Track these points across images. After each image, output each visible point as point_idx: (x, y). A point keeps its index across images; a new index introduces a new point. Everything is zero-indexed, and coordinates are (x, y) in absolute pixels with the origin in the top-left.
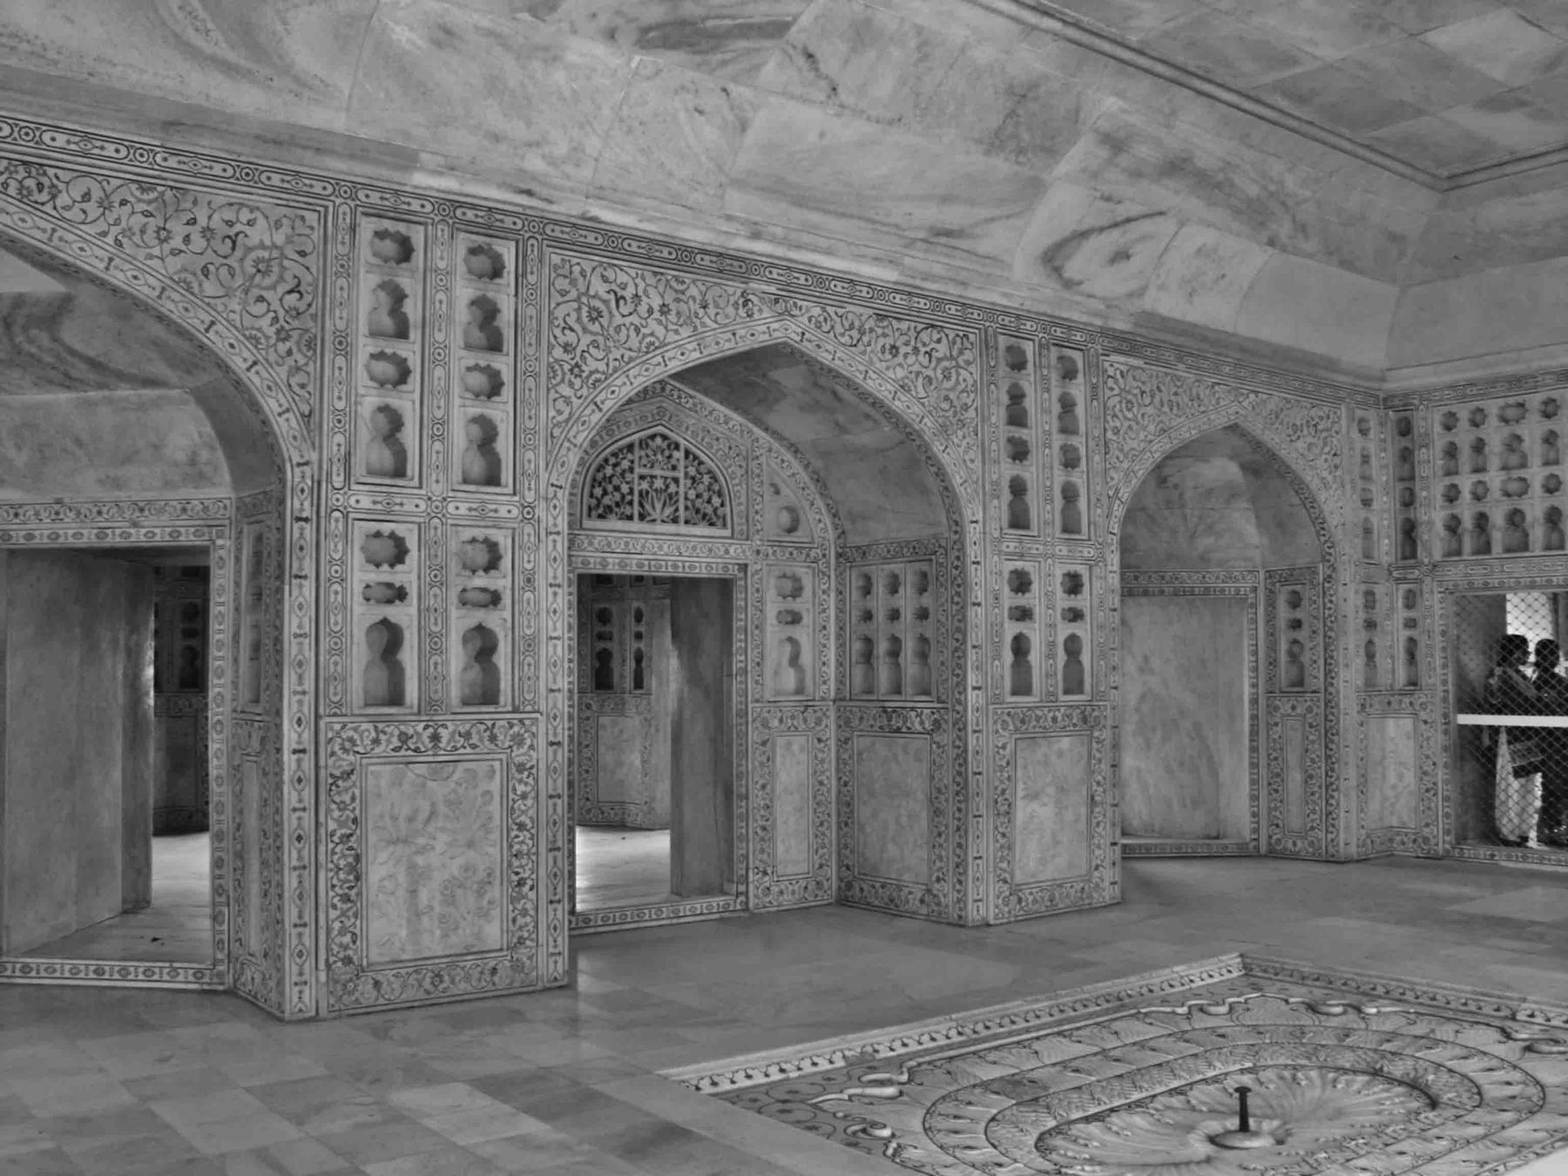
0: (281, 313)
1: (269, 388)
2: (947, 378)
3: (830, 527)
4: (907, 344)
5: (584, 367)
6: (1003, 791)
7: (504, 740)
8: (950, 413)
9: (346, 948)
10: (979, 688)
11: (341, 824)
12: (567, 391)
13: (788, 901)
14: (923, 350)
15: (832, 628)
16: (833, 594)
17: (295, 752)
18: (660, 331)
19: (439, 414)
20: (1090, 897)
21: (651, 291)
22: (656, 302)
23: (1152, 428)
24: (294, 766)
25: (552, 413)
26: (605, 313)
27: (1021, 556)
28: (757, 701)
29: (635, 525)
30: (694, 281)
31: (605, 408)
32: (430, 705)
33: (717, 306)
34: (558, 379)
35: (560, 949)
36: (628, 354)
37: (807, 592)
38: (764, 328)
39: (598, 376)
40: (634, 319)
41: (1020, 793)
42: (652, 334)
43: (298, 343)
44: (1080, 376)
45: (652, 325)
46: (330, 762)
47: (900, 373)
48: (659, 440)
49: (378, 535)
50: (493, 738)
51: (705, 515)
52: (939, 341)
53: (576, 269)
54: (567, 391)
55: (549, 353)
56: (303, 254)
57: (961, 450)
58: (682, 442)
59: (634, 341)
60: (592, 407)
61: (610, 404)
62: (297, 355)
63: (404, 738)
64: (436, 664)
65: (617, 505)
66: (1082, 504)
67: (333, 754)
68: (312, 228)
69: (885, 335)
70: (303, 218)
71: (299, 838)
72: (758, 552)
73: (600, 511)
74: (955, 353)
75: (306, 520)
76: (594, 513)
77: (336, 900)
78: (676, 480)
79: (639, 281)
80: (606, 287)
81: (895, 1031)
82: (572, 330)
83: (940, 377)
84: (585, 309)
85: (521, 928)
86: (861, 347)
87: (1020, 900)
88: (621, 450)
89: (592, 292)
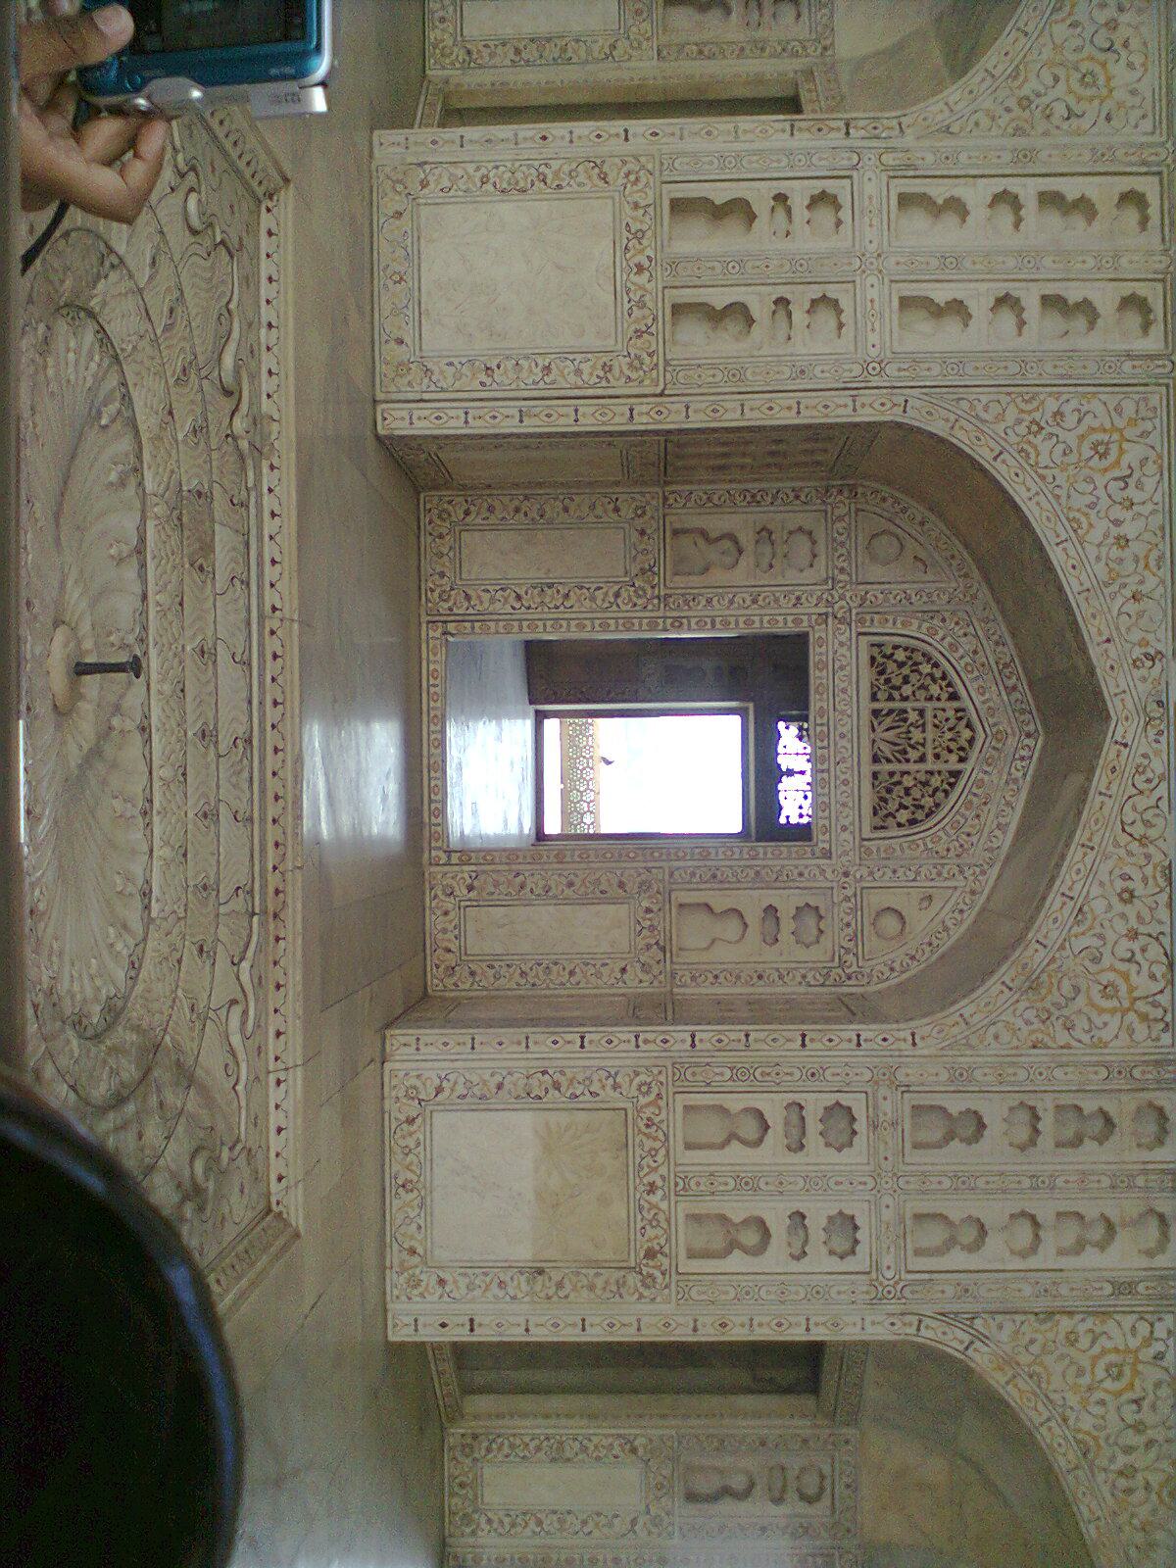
0: (1045, 100)
1: (971, 92)
2: (1106, 996)
3: (887, 984)
4: (1139, 917)
5: (1040, 437)
6: (557, 1086)
7: (637, 346)
8: (1055, 997)
9: (438, 182)
10: (693, 1045)
11: (556, 174)
12: (1011, 414)
13: (434, 922)
14: (1136, 946)
15: (761, 989)
16: (802, 989)
17: (626, 131)
18: (1096, 535)
19: (967, 264)
20: (403, 1269)
21: (1141, 522)
22: (1130, 529)
23: (1087, 1423)
24: (613, 131)
25: (984, 399)
26: (1105, 463)
27: (874, 1126)
28: (671, 875)
29: (867, 705)
30: (1163, 582)
31: (998, 464)
32: (673, 264)
33: (1140, 614)
34: (1022, 406)
35: (418, 424)
36: (1062, 493)
37: (801, 954)
38: (1123, 686)
39: (1033, 455)
40: (1105, 501)
41: (553, 1118)
42: (1091, 525)
43: (1019, 118)
44: (1144, 1262)
45: (1102, 526)
46: (617, 160)
47: (1099, 906)
48: (967, 734)
49: (838, 207)
50: (639, 334)
51: (885, 801)
52: (1153, 977)
53: (1149, 426)
54: (1011, 414)
55: (1050, 394)
56: (1108, 118)
57: (1007, 1017)
58: (967, 767)
59: (1079, 502)
60: (998, 449)
61: (1004, 472)
62: (1007, 117)
63: (639, 235)
64: (713, 268)
65: (888, 681)
66: (957, 1259)
67: (624, 163)
68: (1136, 126)
69: (1145, 880)
70: (1144, 117)
71: (544, 138)
72: (846, 874)
73: (880, 660)
74: (1141, 1006)
75: (848, 133)
76: (876, 650)
77: (483, 171)
78: (922, 759)
79: (1150, 507)
80: (1135, 464)
81: (289, 561)
82: (1080, 421)
83: (1105, 978)
84: (1106, 438)
85: (442, 372)
86: (1124, 839)
87: (411, 1121)
88: (949, 685)
89: (1125, 445)
